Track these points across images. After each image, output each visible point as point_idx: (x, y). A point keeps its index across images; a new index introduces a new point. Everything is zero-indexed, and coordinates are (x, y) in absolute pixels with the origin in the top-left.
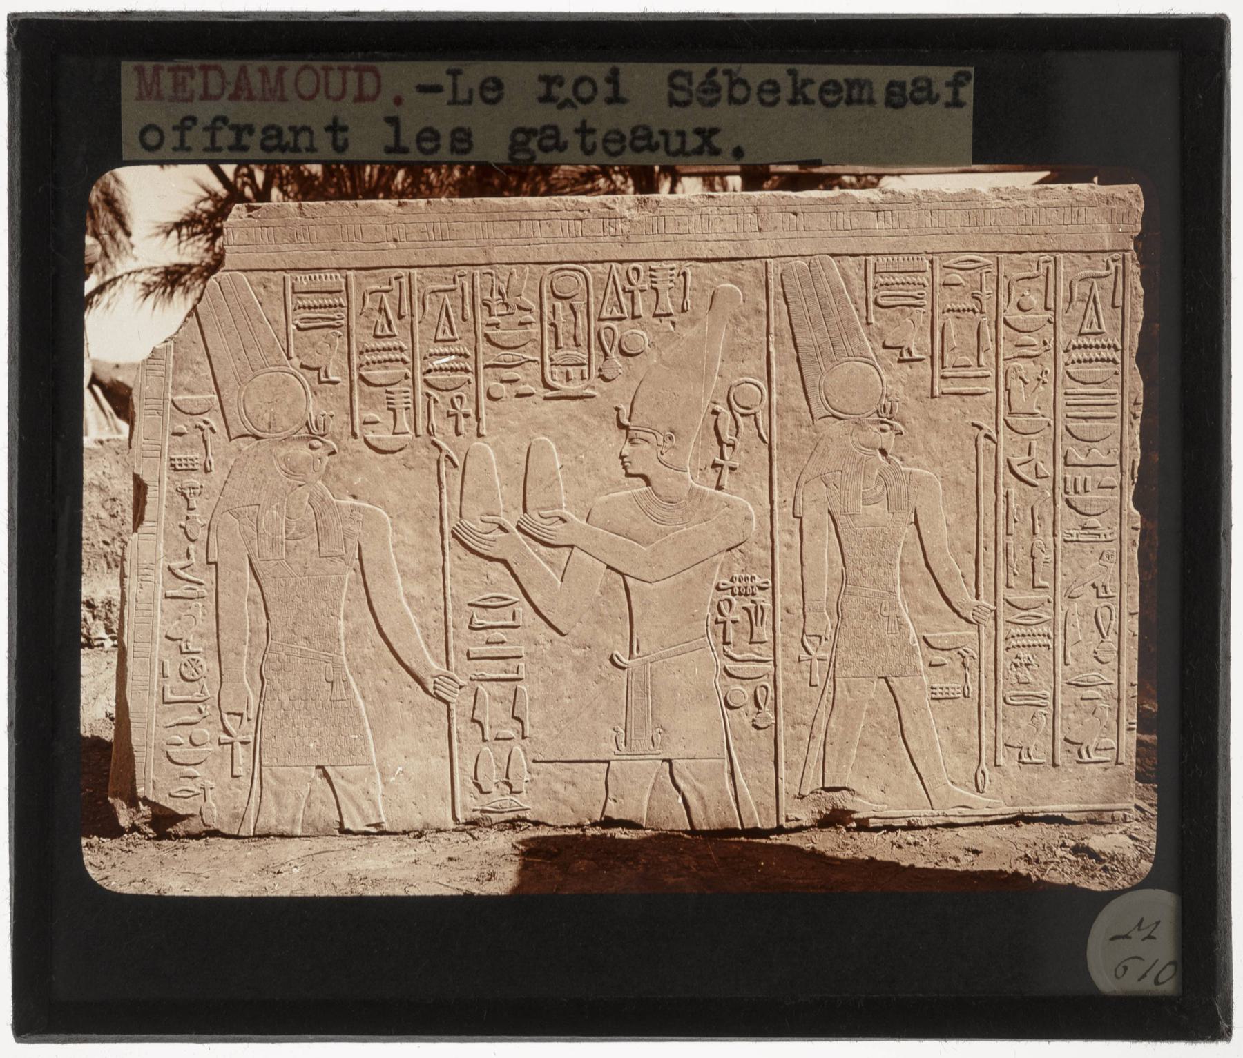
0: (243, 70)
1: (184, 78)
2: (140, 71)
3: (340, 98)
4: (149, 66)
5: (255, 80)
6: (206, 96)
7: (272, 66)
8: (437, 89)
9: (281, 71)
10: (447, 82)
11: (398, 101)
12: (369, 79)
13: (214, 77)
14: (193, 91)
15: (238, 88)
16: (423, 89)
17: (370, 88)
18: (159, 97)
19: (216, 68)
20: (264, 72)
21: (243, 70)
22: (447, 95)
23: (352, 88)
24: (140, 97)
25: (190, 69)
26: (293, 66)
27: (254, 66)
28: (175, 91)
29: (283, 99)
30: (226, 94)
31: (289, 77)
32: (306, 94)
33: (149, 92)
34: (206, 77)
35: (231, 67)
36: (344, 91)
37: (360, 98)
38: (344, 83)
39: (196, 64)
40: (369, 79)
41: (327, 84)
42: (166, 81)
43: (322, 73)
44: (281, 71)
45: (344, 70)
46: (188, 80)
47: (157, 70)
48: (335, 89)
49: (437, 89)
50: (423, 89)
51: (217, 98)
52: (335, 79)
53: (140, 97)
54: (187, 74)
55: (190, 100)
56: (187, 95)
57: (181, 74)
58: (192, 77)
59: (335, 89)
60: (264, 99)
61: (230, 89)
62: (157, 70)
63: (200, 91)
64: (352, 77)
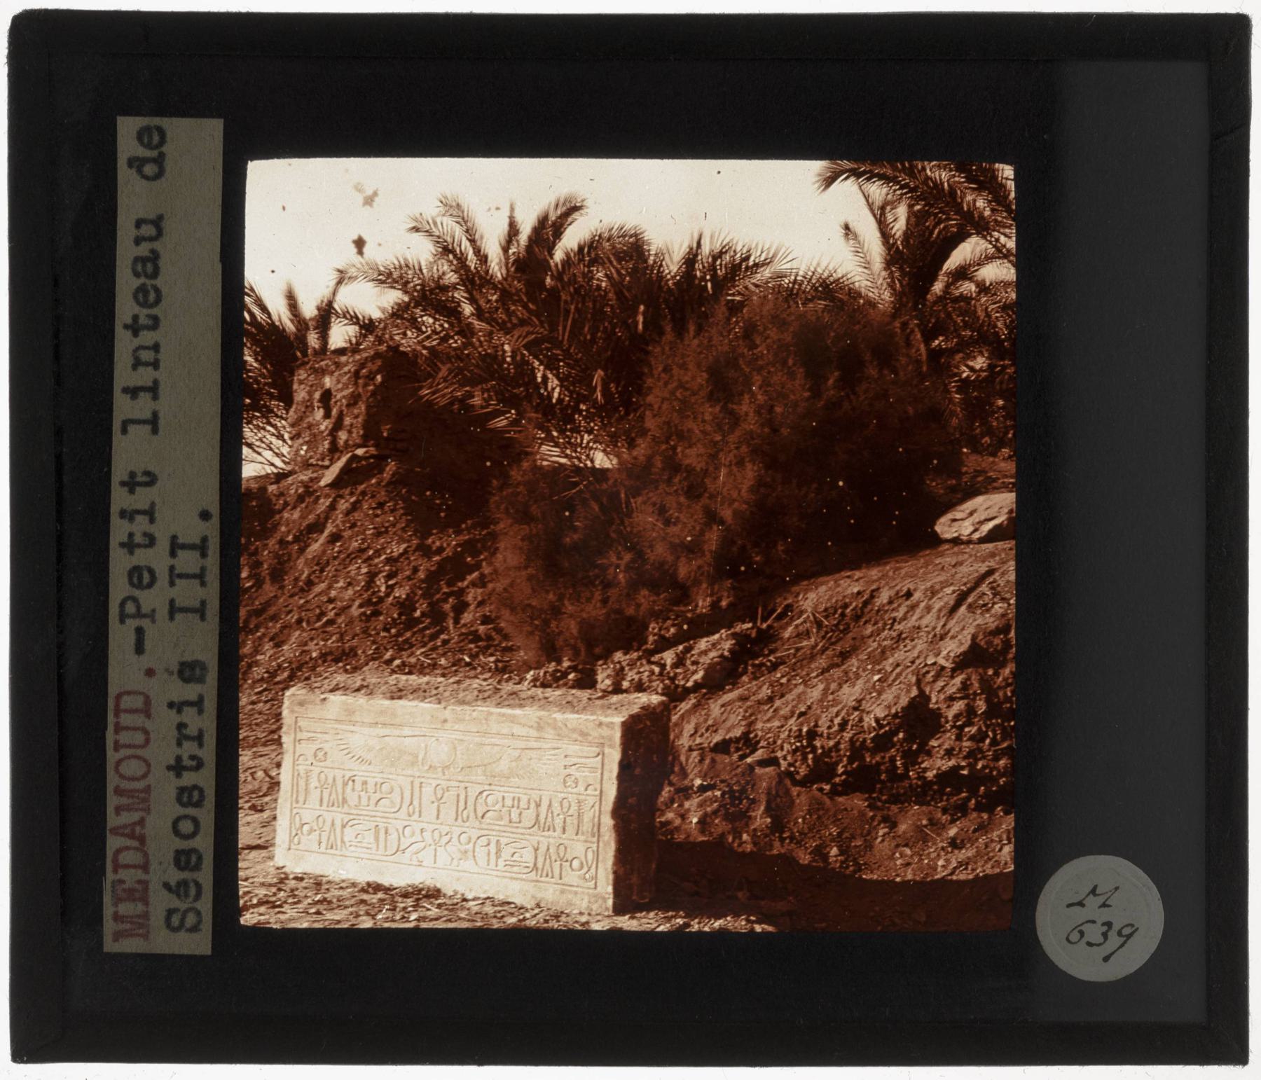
0: (116, 831)
1: (124, 890)
2: (117, 936)
3: (146, 732)
4: (109, 926)
5: (127, 818)
6: (145, 867)
7: (112, 801)
8: (140, 631)
9: (118, 792)
10: (132, 624)
11: (150, 673)
12: (127, 702)
14: (139, 882)
16: (139, 649)
18: (146, 916)
19: (115, 861)
20: (118, 810)
21: (116, 831)
22: (145, 623)
23: (139, 720)
24: (146, 937)
26: (112, 780)
27: (112, 820)
29: (148, 789)
32: (144, 769)
33: (141, 924)
34: (127, 866)
35: (113, 843)
37: (146, 711)
39: (110, 876)
40: (127, 702)
41: (129, 746)
42: (125, 908)
43: (124, 752)
44: (118, 792)
45: (118, 728)
46: (126, 886)
47: (117, 917)
48: (139, 738)
49: (140, 631)
50: (139, 649)
51: (146, 855)
52: (124, 738)
53: (146, 937)
55: (145, 883)
56: (139, 887)
58: (122, 882)
59: (139, 738)
60: (148, 810)
61: (135, 843)
62: (117, 917)
63: (140, 875)
64: (126, 719)
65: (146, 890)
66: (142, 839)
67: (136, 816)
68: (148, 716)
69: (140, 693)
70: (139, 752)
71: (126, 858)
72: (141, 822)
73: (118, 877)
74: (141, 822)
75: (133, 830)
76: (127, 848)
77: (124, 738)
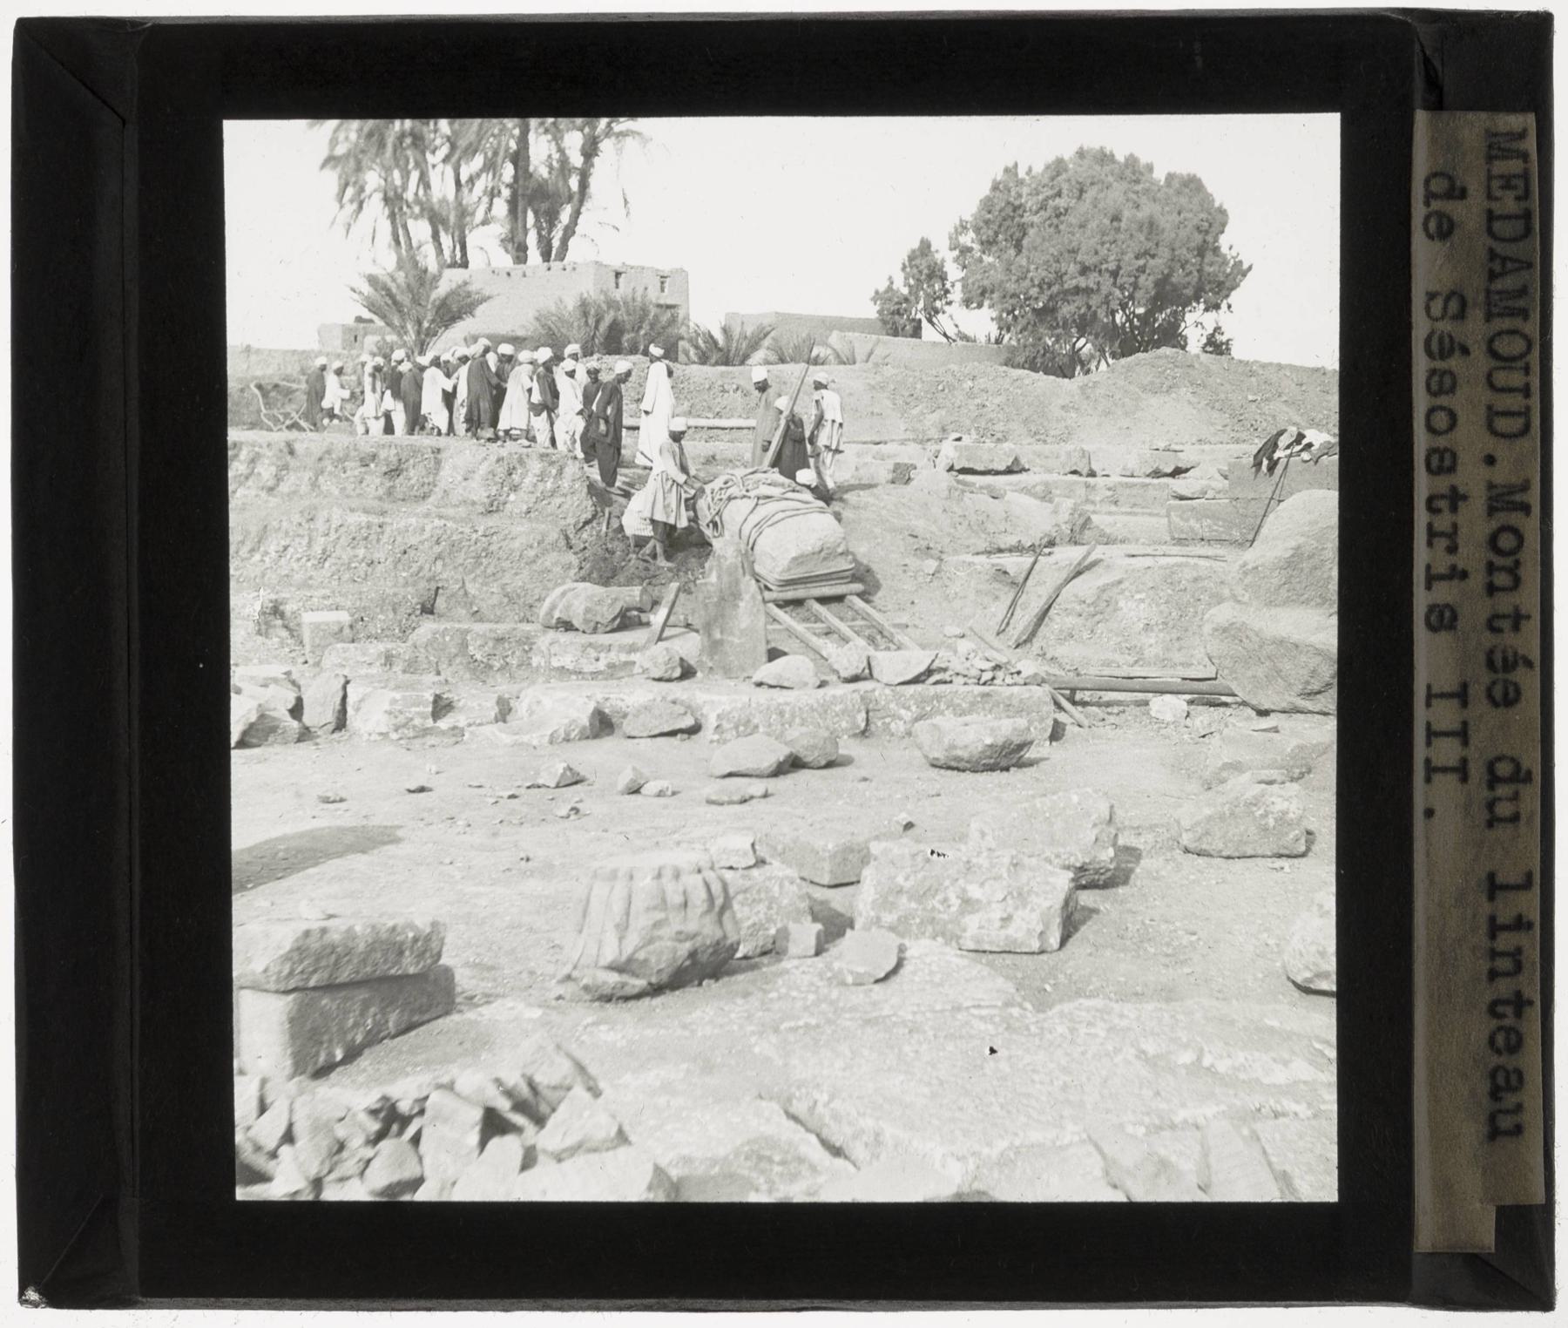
1: (1515, 188)
3: (1492, 386)
12: (1515, 424)
13: (1516, 227)
14: (1497, 199)
15: (1504, 259)
17: (1502, 424)
18: (1490, 159)
25: (1526, 195)
28: (1502, 177)
30: (1490, 242)
31: (1517, 323)
34: (1517, 217)
36: (1503, 390)
37: (1492, 413)
38: (1511, 390)
42: (1515, 166)
48: (1501, 378)
51: (1490, 231)
53: (1491, 134)
54: (1520, 192)
55: (1490, 197)
56: (1498, 193)
57: (1520, 183)
59: (1501, 378)
60: (1488, 292)
61: (1500, 248)
63: (1497, 208)
65: (1489, 187)
66: (1492, 255)
67: (1498, 285)
68: (1490, 408)
69: (1503, 436)
70: (1499, 364)
71: (1516, 227)
72: (1492, 276)
73: (1523, 204)
74: (1492, 276)
75: (1503, 265)
76: (1514, 240)
77: (1516, 379)
